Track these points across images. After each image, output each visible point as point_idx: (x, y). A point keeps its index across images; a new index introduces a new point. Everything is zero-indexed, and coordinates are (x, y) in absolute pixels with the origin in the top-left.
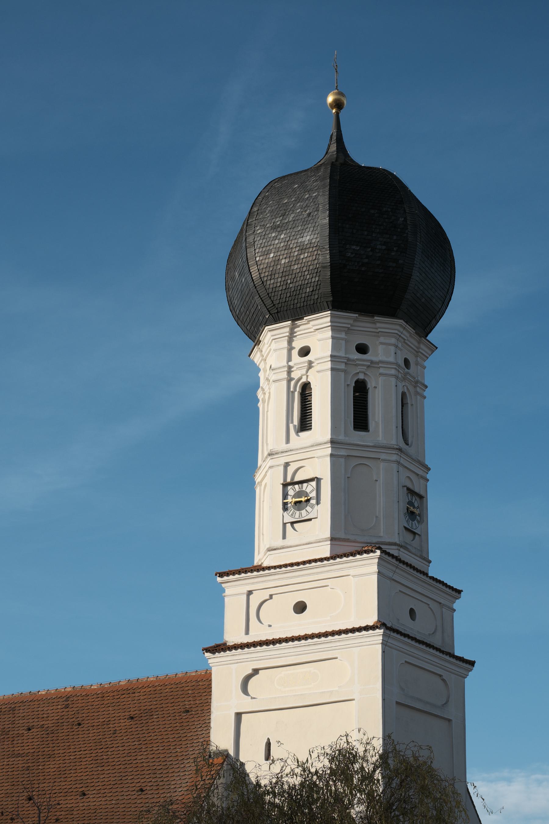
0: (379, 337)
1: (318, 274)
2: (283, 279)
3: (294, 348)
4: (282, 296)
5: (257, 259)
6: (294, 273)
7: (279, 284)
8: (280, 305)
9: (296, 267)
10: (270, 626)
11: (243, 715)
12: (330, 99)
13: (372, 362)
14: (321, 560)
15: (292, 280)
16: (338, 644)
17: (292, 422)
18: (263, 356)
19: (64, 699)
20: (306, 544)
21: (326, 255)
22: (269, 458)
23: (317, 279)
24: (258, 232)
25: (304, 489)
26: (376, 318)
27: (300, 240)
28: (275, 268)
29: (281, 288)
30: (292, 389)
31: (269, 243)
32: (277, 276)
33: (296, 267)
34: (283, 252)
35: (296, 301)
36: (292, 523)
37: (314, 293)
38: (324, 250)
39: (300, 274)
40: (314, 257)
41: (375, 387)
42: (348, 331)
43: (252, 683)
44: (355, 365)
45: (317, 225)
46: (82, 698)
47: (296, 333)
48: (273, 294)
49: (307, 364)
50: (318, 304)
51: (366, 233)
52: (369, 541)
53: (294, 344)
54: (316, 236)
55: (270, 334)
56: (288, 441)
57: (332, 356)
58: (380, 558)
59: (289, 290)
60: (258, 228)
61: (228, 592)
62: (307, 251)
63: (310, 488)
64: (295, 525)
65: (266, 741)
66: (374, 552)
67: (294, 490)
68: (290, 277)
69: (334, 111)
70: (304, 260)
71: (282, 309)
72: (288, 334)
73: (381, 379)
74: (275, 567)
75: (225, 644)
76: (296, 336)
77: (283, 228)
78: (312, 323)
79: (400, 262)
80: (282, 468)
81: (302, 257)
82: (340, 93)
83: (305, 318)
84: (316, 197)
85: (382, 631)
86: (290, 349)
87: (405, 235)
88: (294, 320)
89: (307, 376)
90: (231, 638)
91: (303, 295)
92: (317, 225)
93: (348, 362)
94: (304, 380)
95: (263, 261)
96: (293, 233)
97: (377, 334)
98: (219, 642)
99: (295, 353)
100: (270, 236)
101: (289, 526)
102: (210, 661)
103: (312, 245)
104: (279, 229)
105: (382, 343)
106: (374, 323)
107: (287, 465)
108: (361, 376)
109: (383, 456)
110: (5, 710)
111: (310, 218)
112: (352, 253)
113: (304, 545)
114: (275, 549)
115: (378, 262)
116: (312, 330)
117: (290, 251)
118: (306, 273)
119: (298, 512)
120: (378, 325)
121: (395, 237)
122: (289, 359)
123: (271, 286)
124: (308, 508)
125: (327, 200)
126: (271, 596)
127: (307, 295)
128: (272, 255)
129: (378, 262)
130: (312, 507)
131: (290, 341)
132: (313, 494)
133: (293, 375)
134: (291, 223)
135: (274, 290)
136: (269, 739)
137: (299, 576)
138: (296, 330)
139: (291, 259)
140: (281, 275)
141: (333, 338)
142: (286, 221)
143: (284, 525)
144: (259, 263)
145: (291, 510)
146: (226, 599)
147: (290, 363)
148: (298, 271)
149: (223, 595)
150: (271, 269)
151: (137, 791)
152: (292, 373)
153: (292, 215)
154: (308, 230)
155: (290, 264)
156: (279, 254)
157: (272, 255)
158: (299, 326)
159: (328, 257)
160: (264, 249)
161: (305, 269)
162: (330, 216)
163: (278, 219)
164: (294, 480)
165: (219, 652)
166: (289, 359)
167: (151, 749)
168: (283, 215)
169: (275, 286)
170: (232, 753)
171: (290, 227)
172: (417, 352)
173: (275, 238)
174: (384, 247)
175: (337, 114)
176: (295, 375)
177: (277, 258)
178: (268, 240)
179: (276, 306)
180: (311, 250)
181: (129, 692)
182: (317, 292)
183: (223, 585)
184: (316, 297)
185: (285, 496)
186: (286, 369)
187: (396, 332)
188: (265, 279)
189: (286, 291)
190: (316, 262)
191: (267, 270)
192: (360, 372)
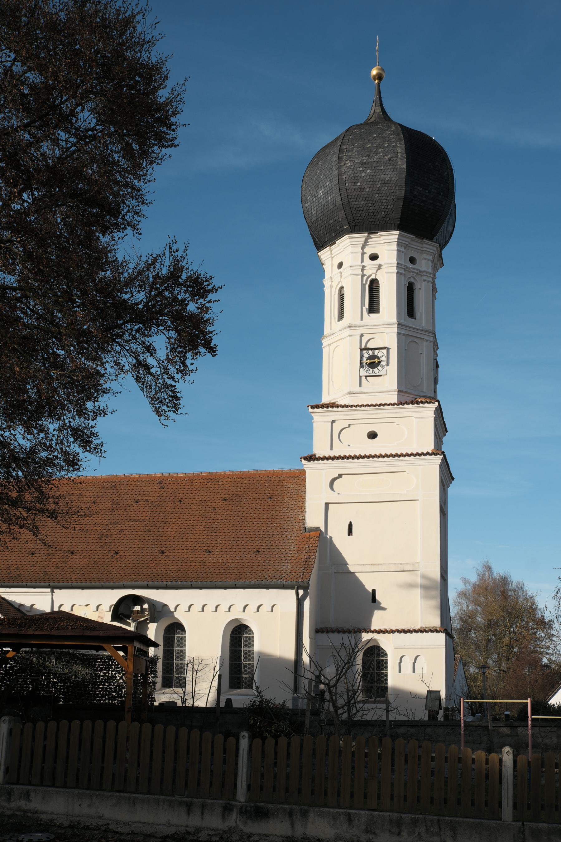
0: (422, 253)
1: (393, 203)
2: (366, 202)
3: (366, 253)
4: (362, 214)
5: (347, 185)
6: (375, 199)
7: (361, 206)
8: (358, 221)
9: (377, 195)
10: (349, 446)
11: (330, 505)
12: (374, 72)
13: (420, 271)
14: (393, 405)
15: (372, 204)
16: (407, 462)
17: (364, 306)
18: (332, 254)
19: (158, 482)
20: (379, 392)
22: (348, 329)
23: (392, 206)
24: (348, 165)
25: (376, 354)
26: (424, 240)
27: (382, 176)
28: (360, 194)
29: (362, 209)
30: (364, 282)
31: (357, 175)
32: (361, 199)
33: (377, 195)
34: (368, 183)
35: (372, 220)
36: (366, 377)
37: (387, 216)
38: (401, 187)
39: (379, 201)
40: (392, 191)
41: (420, 289)
42: (406, 246)
43: (336, 483)
44: (409, 271)
45: (396, 168)
46: (174, 482)
47: (368, 242)
48: (355, 212)
49: (378, 266)
50: (388, 225)
51: (426, 179)
52: (419, 394)
53: (365, 250)
54: (395, 176)
55: (349, 240)
56: (362, 319)
57: (398, 263)
58: (436, 408)
59: (369, 211)
60: (348, 162)
61: (315, 419)
62: (387, 185)
63: (381, 354)
64: (367, 378)
65: (349, 523)
66: (434, 403)
67: (368, 354)
68: (371, 202)
69: (376, 82)
70: (384, 192)
71: (359, 224)
72: (363, 243)
73: (424, 284)
74: (356, 406)
75: (315, 455)
76: (368, 245)
77: (369, 166)
78: (382, 237)
79: (444, 203)
80: (359, 337)
81: (383, 189)
82: (382, 69)
83: (379, 233)
84: (394, 147)
85: (442, 456)
86: (363, 254)
87: (448, 185)
88: (369, 234)
89: (376, 275)
90: (319, 453)
91: (378, 217)
92: (396, 168)
93: (407, 269)
94: (373, 277)
95: (352, 187)
96: (377, 171)
97: (422, 252)
98: (311, 454)
99: (366, 257)
100: (358, 169)
101: (363, 378)
103: (392, 182)
104: (365, 166)
105: (425, 259)
106: (422, 244)
107: (362, 335)
108: (412, 280)
109: (426, 337)
110: (107, 486)
111: (391, 162)
112: (417, 192)
113: (377, 392)
114: (354, 394)
115: (431, 201)
116: (382, 242)
117: (374, 183)
118: (384, 201)
119: (371, 370)
120: (425, 245)
121: (442, 185)
122: (362, 261)
123: (355, 206)
124: (379, 367)
125: (404, 150)
126: (349, 426)
127: (381, 217)
128: (359, 184)
129: (431, 201)
130: (383, 367)
131: (363, 248)
132: (384, 358)
133: (365, 272)
134: (376, 163)
135: (357, 209)
136: (351, 522)
137: (373, 414)
138: (369, 240)
139: (374, 189)
140: (364, 199)
141: (398, 250)
142: (371, 160)
143: (360, 377)
144: (348, 188)
146: (314, 424)
147: (363, 264)
148: (378, 198)
149: (313, 421)
150: (357, 194)
151: (255, 552)
152: (364, 271)
153: (376, 157)
154: (389, 170)
155: (373, 192)
156: (365, 183)
157: (359, 184)
158: (372, 238)
159: (403, 192)
160: (353, 178)
161: (384, 198)
162: (407, 162)
163: (364, 158)
165: (314, 461)
166: (362, 261)
167: (252, 523)
169: (358, 206)
170: (323, 529)
171: (374, 165)
172: (435, 267)
173: (362, 172)
174: (436, 191)
175: (379, 83)
176: (367, 272)
177: (363, 187)
178: (356, 172)
179: (356, 221)
180: (390, 185)
181: (213, 481)
182: (390, 216)
183: (312, 414)
184: (388, 219)
185: (362, 357)
186: (361, 268)
187: (434, 252)
188: (352, 200)
189: (367, 211)
190: (393, 194)
191: (354, 194)
192: (412, 277)
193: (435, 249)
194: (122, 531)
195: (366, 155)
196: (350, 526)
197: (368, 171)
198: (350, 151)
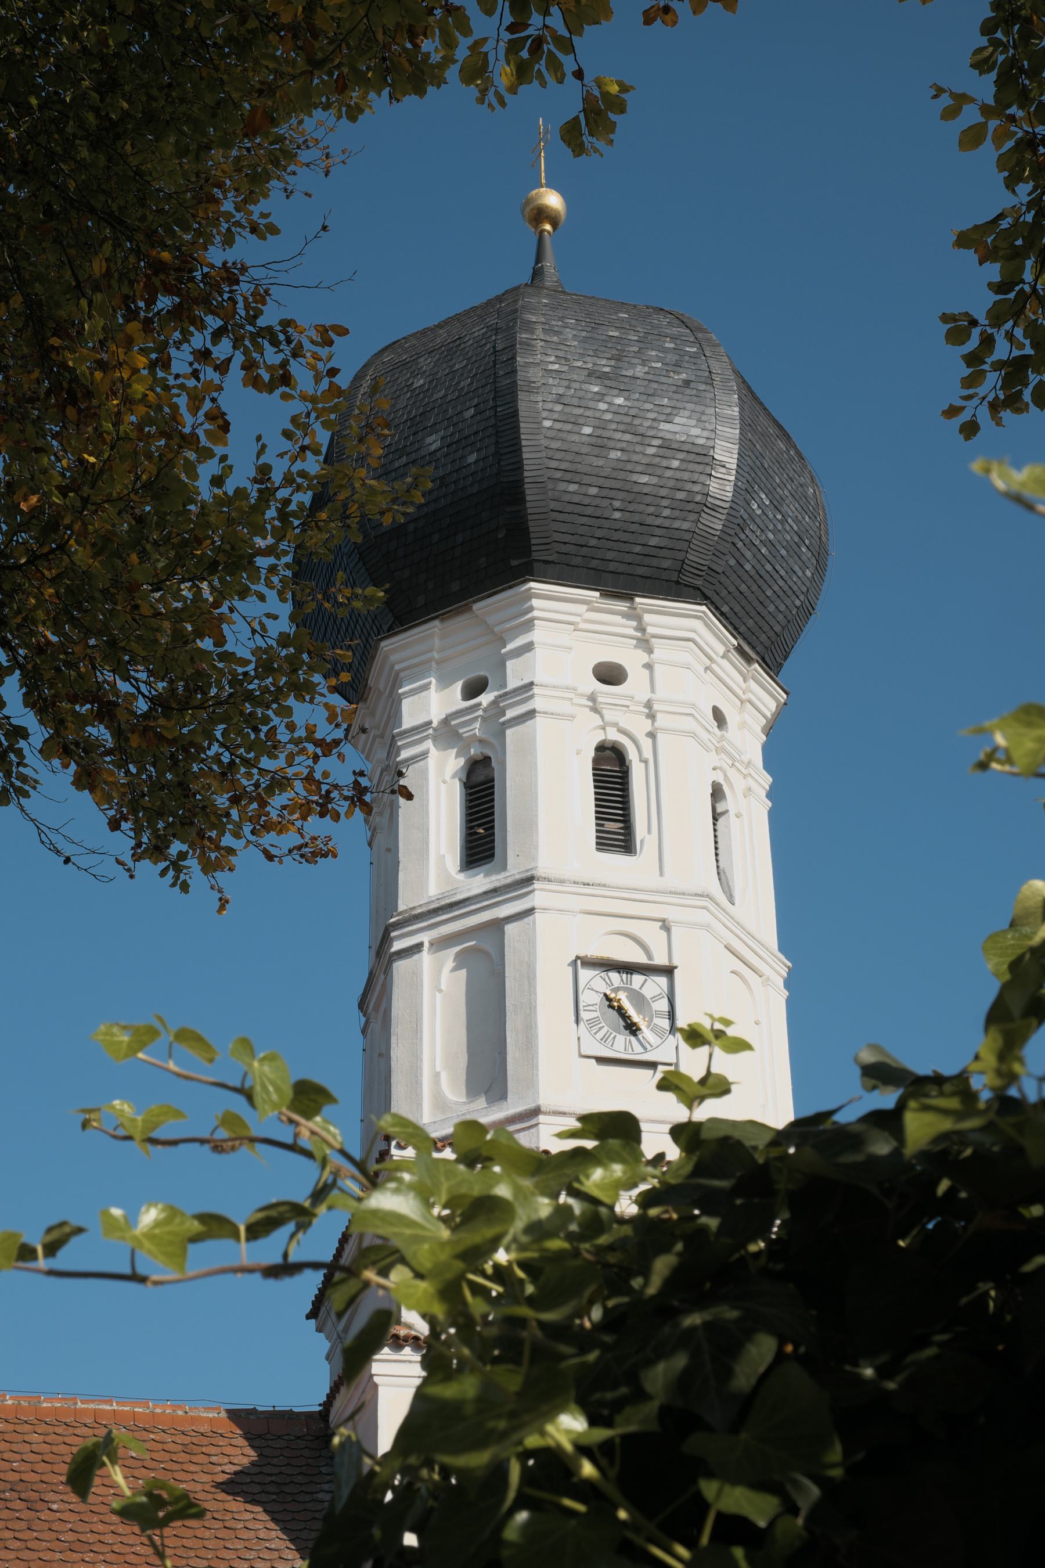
21: (726, 483)
24: (551, 367)
26: (756, 666)
27: (663, 426)
60: (552, 359)
115: (783, 552)
128: (587, 430)
129: (783, 552)
145: (600, 1028)
159: (730, 488)
192: (720, 768)
193: (773, 706)
197: (620, 401)
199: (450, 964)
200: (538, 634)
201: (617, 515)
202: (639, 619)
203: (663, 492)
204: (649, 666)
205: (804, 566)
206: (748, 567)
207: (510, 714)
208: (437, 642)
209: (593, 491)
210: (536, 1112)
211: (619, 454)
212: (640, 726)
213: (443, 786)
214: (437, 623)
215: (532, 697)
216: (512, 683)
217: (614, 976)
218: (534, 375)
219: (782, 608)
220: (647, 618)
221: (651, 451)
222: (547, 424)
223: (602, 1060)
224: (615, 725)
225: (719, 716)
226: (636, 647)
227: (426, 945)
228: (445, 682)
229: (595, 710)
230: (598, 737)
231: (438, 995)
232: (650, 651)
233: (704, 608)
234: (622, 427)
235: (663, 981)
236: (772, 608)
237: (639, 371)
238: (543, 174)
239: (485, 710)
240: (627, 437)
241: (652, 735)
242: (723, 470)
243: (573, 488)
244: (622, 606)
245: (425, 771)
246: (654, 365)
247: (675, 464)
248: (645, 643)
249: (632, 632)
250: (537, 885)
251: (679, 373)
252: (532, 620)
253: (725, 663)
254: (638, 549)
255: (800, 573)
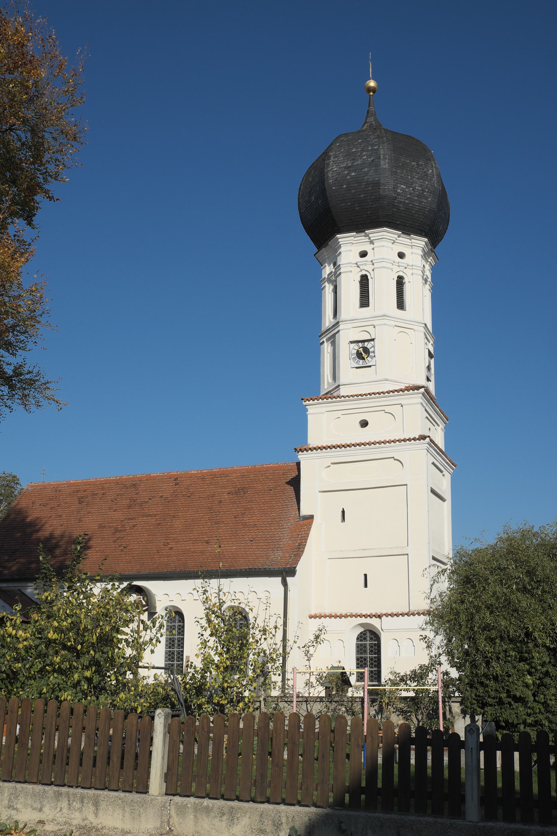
25: (365, 346)
26: (412, 236)
51: (410, 177)
65: (342, 510)
102: (299, 457)
108: (401, 274)
112: (401, 190)
115: (416, 198)
120: (413, 240)
121: (427, 182)
128: (345, 186)
129: (416, 198)
136: (343, 509)
146: (309, 416)
149: (307, 413)
164: (331, 343)
168: (353, 159)
174: (420, 188)
183: (307, 407)
193: (424, 243)
194: (134, 526)
195: (351, 159)
196: (343, 512)
197: (353, 174)
198: (337, 157)
199: (330, 345)
200: (342, 250)
201: (357, 208)
202: (368, 236)
203: (368, 198)
204: (373, 249)
205: (427, 198)
206: (402, 209)
207: (338, 273)
208: (325, 253)
209: (349, 204)
210: (339, 386)
211: (354, 191)
212: (369, 268)
213: (330, 294)
214: (323, 249)
215: (340, 268)
216: (338, 264)
217: (360, 344)
218: (330, 175)
219: (421, 214)
220: (370, 235)
221: (363, 187)
222: (334, 188)
223: (357, 368)
224: (364, 270)
225: (401, 255)
226: (370, 244)
227: (325, 341)
228: (329, 265)
229: (358, 267)
230: (361, 274)
231: (328, 354)
232: (373, 244)
233: (385, 228)
234: (354, 182)
235: (372, 342)
236: (417, 215)
237: (359, 162)
238: (371, 74)
239: (334, 272)
240: (356, 185)
241: (373, 270)
242: (384, 186)
243: (344, 204)
244: (363, 234)
245: (325, 292)
246: (364, 158)
247: (370, 188)
248: (372, 242)
249: (368, 240)
250: (340, 323)
251: (371, 158)
252: (340, 245)
253: (400, 238)
254: (365, 216)
255: (426, 201)
